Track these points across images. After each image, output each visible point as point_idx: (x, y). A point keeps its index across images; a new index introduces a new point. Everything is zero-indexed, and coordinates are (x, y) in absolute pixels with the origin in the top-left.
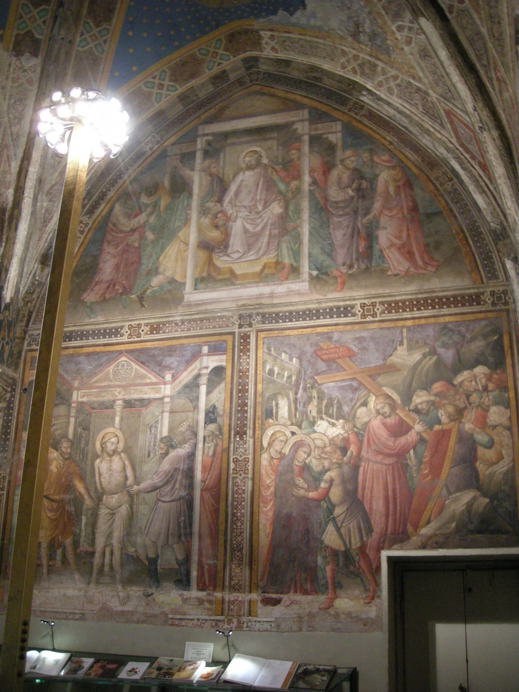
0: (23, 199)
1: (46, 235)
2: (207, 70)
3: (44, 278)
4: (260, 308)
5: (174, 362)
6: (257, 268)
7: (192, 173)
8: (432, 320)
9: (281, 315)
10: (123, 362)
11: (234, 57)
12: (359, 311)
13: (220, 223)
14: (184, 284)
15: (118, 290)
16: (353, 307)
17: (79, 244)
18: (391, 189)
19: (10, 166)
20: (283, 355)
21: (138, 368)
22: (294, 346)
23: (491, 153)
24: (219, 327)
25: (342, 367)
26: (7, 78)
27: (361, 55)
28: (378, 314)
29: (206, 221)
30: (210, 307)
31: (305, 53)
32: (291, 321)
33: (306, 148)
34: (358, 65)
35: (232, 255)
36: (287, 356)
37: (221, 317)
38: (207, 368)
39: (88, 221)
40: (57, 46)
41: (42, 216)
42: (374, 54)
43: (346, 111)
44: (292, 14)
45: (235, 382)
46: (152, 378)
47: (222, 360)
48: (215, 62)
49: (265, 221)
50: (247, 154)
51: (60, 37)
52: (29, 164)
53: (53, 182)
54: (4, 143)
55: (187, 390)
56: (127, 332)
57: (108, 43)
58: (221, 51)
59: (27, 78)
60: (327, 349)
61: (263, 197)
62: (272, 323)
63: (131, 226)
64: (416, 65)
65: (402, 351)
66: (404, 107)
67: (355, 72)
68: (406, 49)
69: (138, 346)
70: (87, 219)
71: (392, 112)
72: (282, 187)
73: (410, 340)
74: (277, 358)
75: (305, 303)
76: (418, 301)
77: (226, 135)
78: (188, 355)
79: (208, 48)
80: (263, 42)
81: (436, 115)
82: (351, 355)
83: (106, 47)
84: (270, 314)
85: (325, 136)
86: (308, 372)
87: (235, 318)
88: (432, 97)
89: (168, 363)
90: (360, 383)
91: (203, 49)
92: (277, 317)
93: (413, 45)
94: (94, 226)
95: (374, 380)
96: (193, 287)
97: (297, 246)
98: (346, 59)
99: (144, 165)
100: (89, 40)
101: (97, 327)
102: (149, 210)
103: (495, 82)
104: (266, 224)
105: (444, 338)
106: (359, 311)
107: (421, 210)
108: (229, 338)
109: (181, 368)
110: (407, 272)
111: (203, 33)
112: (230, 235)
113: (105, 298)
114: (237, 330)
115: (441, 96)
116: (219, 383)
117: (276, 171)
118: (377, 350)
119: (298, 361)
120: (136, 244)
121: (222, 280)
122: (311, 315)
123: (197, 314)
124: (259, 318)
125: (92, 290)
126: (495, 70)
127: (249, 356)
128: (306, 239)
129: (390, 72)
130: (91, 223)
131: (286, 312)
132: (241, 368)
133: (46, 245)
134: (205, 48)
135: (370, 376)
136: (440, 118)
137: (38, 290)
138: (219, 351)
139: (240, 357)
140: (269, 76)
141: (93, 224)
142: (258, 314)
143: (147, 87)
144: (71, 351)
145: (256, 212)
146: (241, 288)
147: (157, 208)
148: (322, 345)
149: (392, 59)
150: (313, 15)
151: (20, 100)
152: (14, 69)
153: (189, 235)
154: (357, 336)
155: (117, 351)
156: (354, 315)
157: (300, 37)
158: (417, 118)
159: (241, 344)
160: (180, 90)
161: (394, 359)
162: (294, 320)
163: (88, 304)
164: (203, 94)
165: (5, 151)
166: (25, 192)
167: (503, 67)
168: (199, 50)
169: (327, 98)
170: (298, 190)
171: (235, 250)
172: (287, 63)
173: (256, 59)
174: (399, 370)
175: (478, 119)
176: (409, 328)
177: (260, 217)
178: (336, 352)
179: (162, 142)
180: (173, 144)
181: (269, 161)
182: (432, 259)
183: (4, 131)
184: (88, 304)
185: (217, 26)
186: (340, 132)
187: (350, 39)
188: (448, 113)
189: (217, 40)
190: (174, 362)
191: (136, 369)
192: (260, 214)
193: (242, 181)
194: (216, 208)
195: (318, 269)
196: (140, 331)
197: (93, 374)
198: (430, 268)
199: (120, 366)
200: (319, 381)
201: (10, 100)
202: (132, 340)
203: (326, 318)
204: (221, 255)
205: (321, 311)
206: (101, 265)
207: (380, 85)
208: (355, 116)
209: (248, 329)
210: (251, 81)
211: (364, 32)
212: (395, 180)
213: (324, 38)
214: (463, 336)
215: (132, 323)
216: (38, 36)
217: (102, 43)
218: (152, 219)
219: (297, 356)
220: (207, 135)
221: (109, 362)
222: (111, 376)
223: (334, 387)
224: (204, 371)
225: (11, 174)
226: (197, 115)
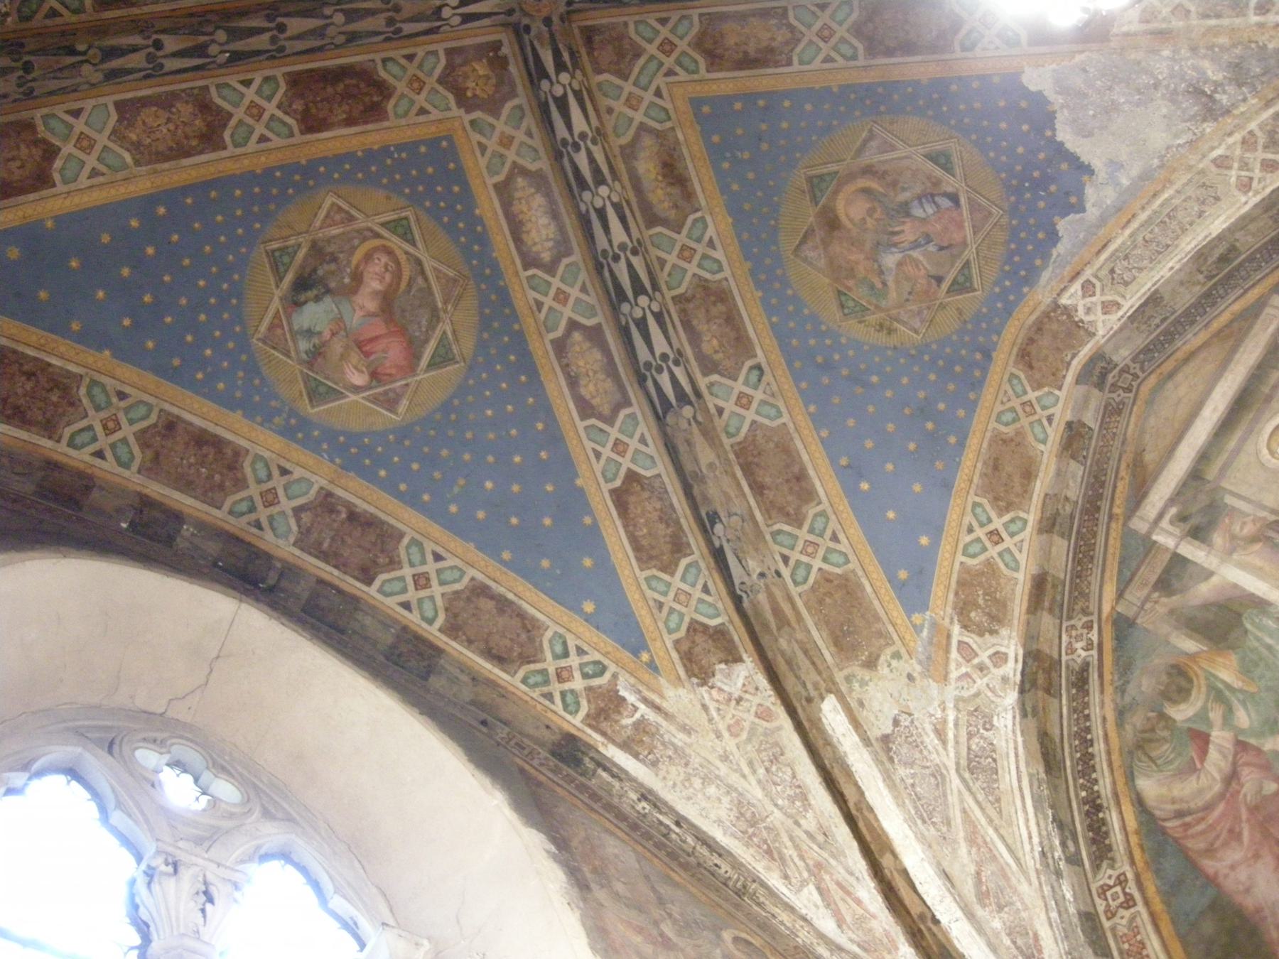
0: (945, 934)
2: (1042, 447)
7: (1214, 580)
11: (1060, 388)
17: (1150, 928)
19: (859, 902)
27: (1253, 126)
34: (1266, 147)
39: (1115, 873)
40: (762, 597)
41: (1015, 952)
42: (1271, 96)
44: (1082, 209)
51: (755, 576)
53: (972, 869)
54: (811, 863)
57: (841, 536)
58: (1032, 395)
59: (753, 709)
63: (1217, 776)
70: (1110, 872)
77: (1196, 475)
79: (1008, 405)
80: (1081, 314)
83: (844, 546)
91: (1002, 412)
94: (1140, 864)
98: (1236, 165)
99: (1107, 677)
100: (804, 559)
102: (1216, 715)
111: (978, 385)
130: (1127, 869)
134: (1001, 408)
140: (1146, 355)
143: (974, 556)
147: (1227, 693)
150: (1115, 165)
151: (775, 759)
152: (719, 710)
157: (1128, 232)
160: (1032, 517)
164: (1075, 491)
165: (827, 877)
166: (938, 916)
168: (998, 420)
172: (1154, 300)
173: (1098, 357)
179: (1095, 618)
180: (1120, 595)
183: (791, 838)
185: (987, 355)
187: (1208, 127)
189: (1010, 381)
201: (754, 772)
206: (1249, 903)
210: (1129, 390)
211: (1217, 85)
216: (713, 622)
217: (832, 545)
218: (1243, 718)
220: (1161, 516)
225: (874, 916)
226: (1103, 517)
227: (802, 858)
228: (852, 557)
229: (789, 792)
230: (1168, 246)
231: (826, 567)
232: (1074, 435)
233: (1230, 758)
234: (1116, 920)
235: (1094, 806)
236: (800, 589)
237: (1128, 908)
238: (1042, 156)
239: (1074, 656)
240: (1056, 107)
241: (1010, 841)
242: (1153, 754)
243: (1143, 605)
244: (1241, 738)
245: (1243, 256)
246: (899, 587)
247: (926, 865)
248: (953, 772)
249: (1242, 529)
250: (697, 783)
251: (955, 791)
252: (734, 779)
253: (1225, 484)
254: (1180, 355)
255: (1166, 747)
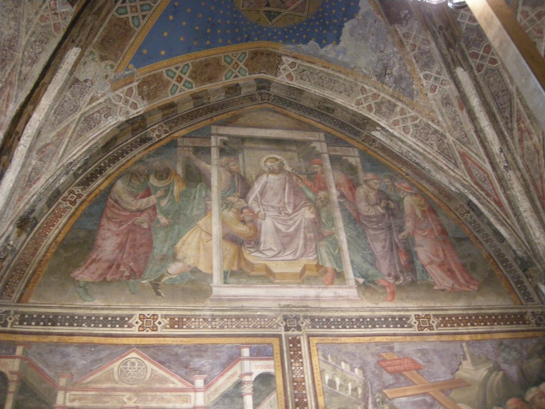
0: (17, 145)
1: (29, 197)
2: (224, 79)
3: (19, 244)
4: (307, 311)
5: (206, 364)
6: (298, 269)
7: (208, 166)
8: (487, 336)
9: (332, 320)
10: (133, 360)
11: (250, 74)
12: (415, 323)
13: (247, 219)
14: (211, 275)
15: (124, 272)
16: (408, 318)
17: (69, 215)
18: (418, 212)
19: (7, 106)
20: (343, 364)
21: (155, 368)
22: (354, 355)
23: (516, 189)
24: (261, 327)
25: (411, 381)
26: (36, 13)
27: (382, 95)
28: (435, 327)
29: (230, 214)
30: (246, 304)
31: (321, 86)
32: (344, 327)
33: (328, 164)
34: (376, 103)
35: (264, 252)
36: (348, 366)
37: (261, 317)
38: (250, 374)
39: (80, 192)
41: (28, 175)
42: (395, 96)
43: (360, 141)
44: (322, 46)
45: (289, 393)
46: (176, 382)
47: (269, 367)
48: (233, 73)
49: (297, 223)
50: (267, 159)
52: (34, 109)
54: (10, 79)
55: (227, 401)
56: (137, 323)
57: (146, 19)
58: (241, 65)
59: (56, 22)
60: (391, 360)
61: (292, 200)
62: (323, 328)
63: (138, 206)
64: (437, 110)
65: (467, 365)
66: (418, 145)
67: (370, 108)
68: (430, 95)
69: (153, 341)
70: (80, 190)
71: (405, 148)
72: (310, 195)
73: (472, 355)
74: (336, 367)
75: (357, 310)
76: (470, 316)
77: (243, 139)
78: (224, 358)
79: (233, 57)
80: (282, 67)
81: (451, 156)
82: (418, 368)
83: (143, 22)
84: (320, 318)
85: (344, 158)
86: (375, 385)
87: (279, 319)
88: (449, 139)
89: (197, 366)
90: (434, 399)
91: (229, 57)
92: (328, 322)
93: (436, 92)
94: (89, 199)
95: (447, 395)
96: (223, 281)
97: (337, 252)
98: (365, 96)
99: (151, 149)
100: (129, 9)
101: (94, 312)
102: (159, 193)
103: (516, 133)
104: (299, 226)
105: (504, 354)
106: (415, 323)
107: (450, 235)
108: (275, 341)
109: (216, 372)
110: (453, 288)
111: (235, 42)
112: (260, 232)
113: (105, 279)
114: (283, 333)
115: (457, 139)
116: (268, 394)
117: (301, 179)
118: (443, 363)
119: (361, 372)
120: (145, 226)
121: (257, 277)
122: (365, 323)
123: (230, 310)
124: (308, 321)
125: (87, 268)
126: (517, 121)
127: (302, 363)
128: (345, 246)
129: (409, 112)
131: (337, 317)
132: (294, 376)
133: (27, 207)
134: (230, 55)
135: (442, 391)
136: (454, 158)
137: (10, 258)
138: (263, 355)
139: (291, 364)
140: (279, 99)
141: (88, 196)
142: (305, 317)
143: (168, 75)
144: (55, 339)
145: (286, 214)
146: (282, 287)
147: (170, 193)
148: (384, 355)
149: (414, 102)
150: (344, 51)
151: (42, 42)
152: (47, 8)
153: (211, 225)
154: (419, 348)
155: (125, 345)
156: (410, 326)
157: (321, 69)
158: (431, 157)
159: (290, 349)
160: (195, 89)
161: (460, 374)
162: (348, 327)
163: (82, 284)
164: (214, 100)
165: (8, 89)
166: (22, 139)
167: (529, 118)
168: (225, 56)
169: (341, 128)
170: (327, 201)
171: (268, 248)
172: (301, 91)
173: (269, 82)
174: (469, 385)
175: (504, 159)
176: (468, 342)
177: (291, 219)
178: (400, 364)
179: (170, 132)
180: (184, 137)
181: (292, 170)
182: (472, 278)
183: (14, 66)
184: (82, 284)
185: (248, 40)
186: (358, 157)
187: (374, 79)
188: (463, 155)
189: (243, 53)
190: (206, 364)
191: (152, 370)
192: (291, 216)
193: (266, 183)
194: (239, 203)
195: (363, 277)
196: (156, 323)
197: (88, 371)
198: (472, 287)
199: (129, 364)
200: (389, 396)
201: (31, 36)
202: (145, 333)
203: (382, 327)
204: (252, 250)
205: (376, 319)
206: (99, 242)
207: (396, 123)
208: (369, 146)
209: (296, 332)
210: (262, 100)
212: (419, 205)
213: (347, 74)
214: (520, 353)
215: (145, 313)
217: (140, 17)
218: (164, 203)
219: (359, 366)
221: (112, 358)
222: (116, 377)
223: (407, 402)
224: (247, 378)
225: (5, 116)
226: (210, 115)
227: (9, 75)
228: (140, 27)
229: (32, 55)
230: (323, 86)
231: (130, 19)
232: (234, 89)
233: (147, 207)
234: (64, 203)
235: (100, 171)
236: (115, 14)
237: (71, 204)
238: (335, 21)
239: (152, 133)
240: (357, 17)
241: (68, 149)
242: (132, 180)
243: (185, 146)
244: (157, 206)
245: (332, 115)
246: (139, 52)
247: (38, 123)
248: (80, 113)
249: (232, 165)
250: (12, 15)
251: (74, 118)
252: (23, 30)
253: (245, 151)
254: (285, 111)
255: (138, 183)
